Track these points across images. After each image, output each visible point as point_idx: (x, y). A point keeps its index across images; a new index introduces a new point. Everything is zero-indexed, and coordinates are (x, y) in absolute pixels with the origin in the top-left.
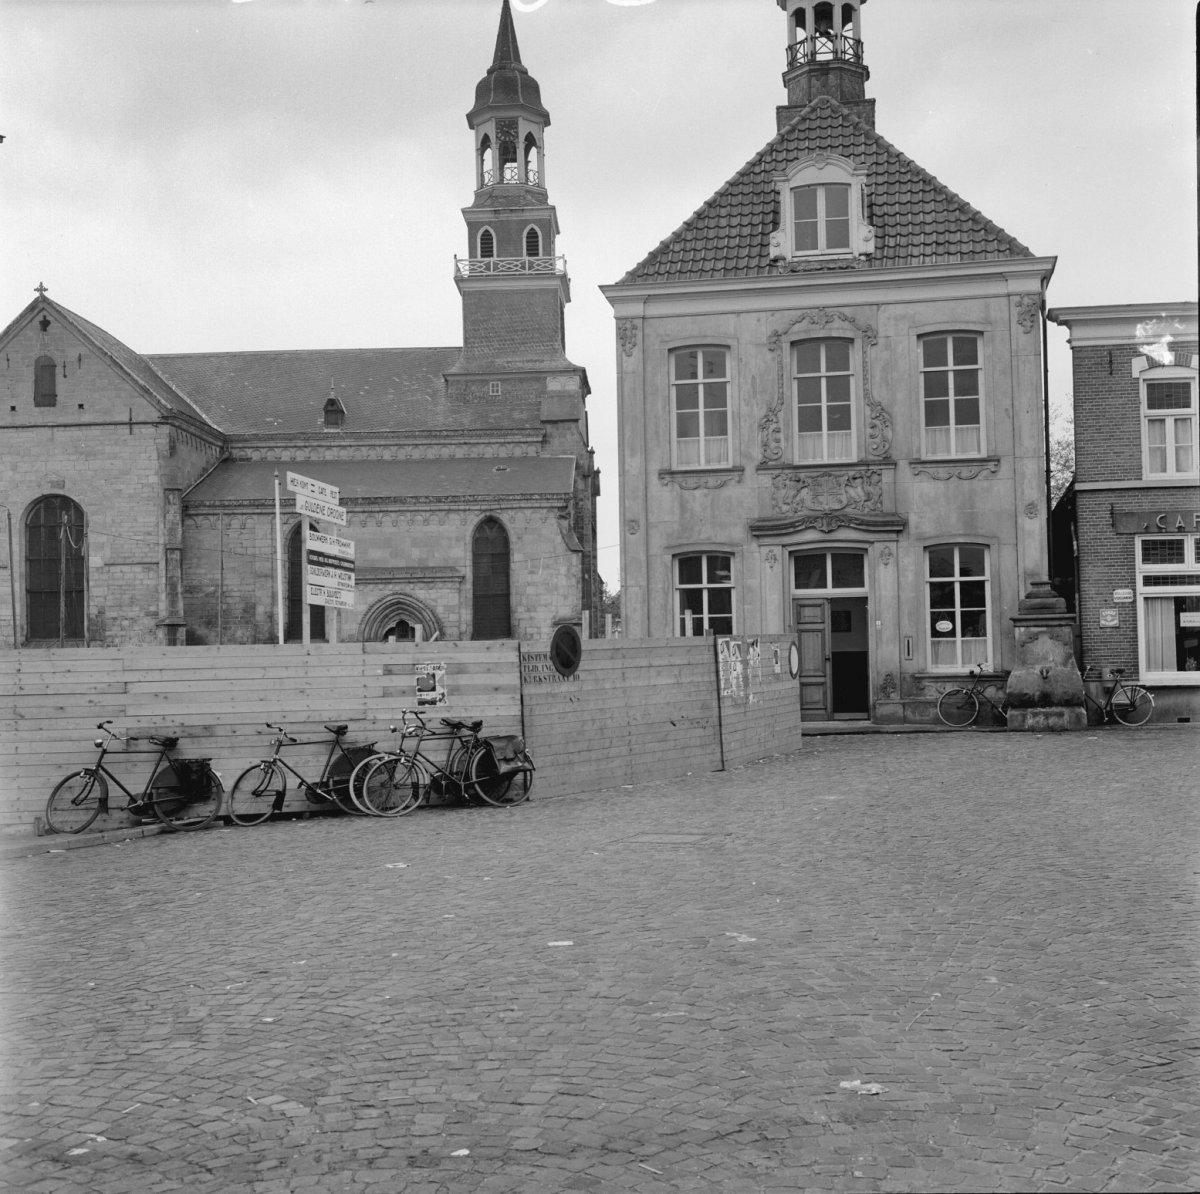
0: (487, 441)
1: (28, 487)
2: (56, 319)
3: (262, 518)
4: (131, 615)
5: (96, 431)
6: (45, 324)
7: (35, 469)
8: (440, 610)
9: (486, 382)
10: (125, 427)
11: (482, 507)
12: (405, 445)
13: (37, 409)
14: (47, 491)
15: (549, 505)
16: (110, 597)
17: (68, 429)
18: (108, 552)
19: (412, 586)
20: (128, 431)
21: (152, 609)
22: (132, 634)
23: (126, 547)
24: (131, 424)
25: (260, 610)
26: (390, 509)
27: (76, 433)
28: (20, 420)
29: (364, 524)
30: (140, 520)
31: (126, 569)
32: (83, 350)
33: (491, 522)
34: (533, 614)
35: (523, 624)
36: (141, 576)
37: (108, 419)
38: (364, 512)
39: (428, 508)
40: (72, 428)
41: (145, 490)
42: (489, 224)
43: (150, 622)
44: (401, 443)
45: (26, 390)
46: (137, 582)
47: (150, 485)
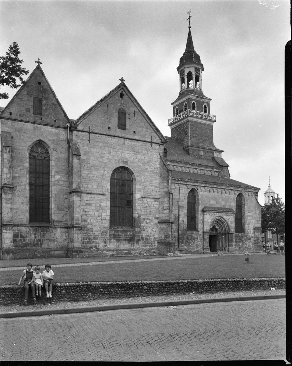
0: (207, 169)
1: (114, 162)
3: (182, 186)
4: (150, 218)
5: (139, 143)
7: (117, 155)
8: (229, 223)
9: (199, 151)
10: (150, 143)
11: (241, 190)
13: (119, 130)
14: (121, 165)
15: (255, 191)
17: (130, 140)
18: (142, 192)
19: (223, 214)
20: (150, 145)
21: (157, 216)
24: (151, 143)
25: (181, 219)
26: (218, 187)
27: (133, 143)
28: (112, 133)
29: (210, 191)
30: (154, 181)
31: (148, 200)
33: (240, 195)
34: (249, 226)
35: (247, 228)
36: (153, 203)
37: (144, 139)
38: (211, 187)
39: (228, 188)
40: (131, 140)
41: (155, 169)
43: (156, 221)
45: (114, 121)
46: (152, 205)
47: (157, 168)
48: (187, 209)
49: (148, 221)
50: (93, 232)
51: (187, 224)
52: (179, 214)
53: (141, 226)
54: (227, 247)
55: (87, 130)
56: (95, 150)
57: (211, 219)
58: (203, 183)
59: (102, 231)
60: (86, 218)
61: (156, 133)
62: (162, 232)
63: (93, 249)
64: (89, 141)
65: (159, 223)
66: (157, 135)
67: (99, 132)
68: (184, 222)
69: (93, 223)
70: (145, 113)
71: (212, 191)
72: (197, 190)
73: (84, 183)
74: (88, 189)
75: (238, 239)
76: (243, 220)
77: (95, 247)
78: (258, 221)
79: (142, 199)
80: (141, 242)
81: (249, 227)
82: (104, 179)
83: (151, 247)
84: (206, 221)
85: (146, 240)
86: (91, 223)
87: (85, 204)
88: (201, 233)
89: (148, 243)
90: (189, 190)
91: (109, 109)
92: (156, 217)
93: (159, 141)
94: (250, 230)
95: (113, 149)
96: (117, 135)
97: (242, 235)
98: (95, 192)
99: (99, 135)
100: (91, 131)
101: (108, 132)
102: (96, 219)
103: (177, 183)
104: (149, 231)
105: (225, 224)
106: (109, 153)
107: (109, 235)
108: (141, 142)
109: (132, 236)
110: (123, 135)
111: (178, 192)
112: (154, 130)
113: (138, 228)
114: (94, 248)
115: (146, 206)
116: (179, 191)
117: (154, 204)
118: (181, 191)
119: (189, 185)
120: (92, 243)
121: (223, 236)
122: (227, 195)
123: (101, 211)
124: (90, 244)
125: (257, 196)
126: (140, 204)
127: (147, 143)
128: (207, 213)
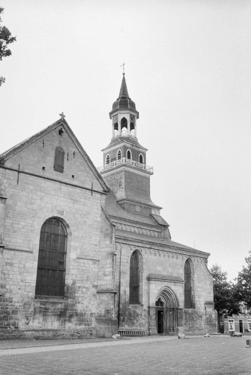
2: (66, 132)
3: (125, 245)
4: (87, 286)
5: (78, 190)
6: (61, 132)
10: (90, 191)
11: (190, 254)
12: (122, 224)
13: (55, 172)
14: (56, 215)
16: (78, 276)
17: (68, 185)
18: (78, 251)
19: (171, 283)
20: (90, 194)
21: (95, 284)
22: (86, 296)
23: (86, 250)
24: (92, 190)
25: (122, 289)
26: (165, 250)
27: (71, 189)
28: (47, 175)
30: (93, 238)
31: (86, 261)
32: (76, 151)
33: (188, 262)
36: (92, 266)
39: (175, 252)
40: (69, 186)
42: (130, 148)
43: (94, 291)
44: (122, 223)
45: (50, 161)
47: (98, 222)
48: (129, 275)
49: (84, 290)
50: (13, 304)
51: (129, 295)
52: (120, 283)
53: (75, 297)
54: (176, 326)
55: (16, 168)
56: (24, 193)
57: (157, 290)
58: (148, 244)
59: (24, 302)
60: (5, 283)
61: (98, 179)
62: (101, 306)
63: (10, 327)
64: (18, 181)
65: (98, 293)
66: (99, 182)
67: (31, 172)
68: (125, 292)
69: (13, 291)
70: (86, 155)
71: (158, 254)
72: (141, 252)
73: (7, 236)
74: (11, 244)
75: (188, 316)
76: (192, 292)
77: (13, 325)
78: (209, 293)
79: (78, 260)
80: (74, 319)
81: (199, 301)
82: (32, 231)
83: (87, 327)
84: (151, 293)
85: (81, 317)
86: (11, 291)
87: (4, 264)
88: (145, 307)
89: (83, 321)
90: (132, 252)
91: (45, 146)
92: (95, 285)
93: (101, 190)
94: (201, 305)
95: (47, 194)
96: (52, 177)
97: (192, 311)
98: (19, 248)
99: (31, 176)
100: (20, 170)
101: (41, 173)
102: (18, 285)
103: (118, 243)
104: (86, 303)
105: (173, 296)
106: (42, 199)
107: (33, 308)
108: (80, 189)
109: (63, 310)
110: (60, 179)
111: (120, 253)
112: (95, 176)
113: (72, 299)
114: (11, 327)
115: (82, 270)
116: (121, 252)
117: (92, 268)
118: (123, 252)
119: (132, 245)
120: (10, 319)
121: (171, 313)
122: (175, 260)
123: (25, 274)
124: (7, 320)
125: (207, 262)
126: (75, 267)
127: (87, 190)
128: (153, 282)
